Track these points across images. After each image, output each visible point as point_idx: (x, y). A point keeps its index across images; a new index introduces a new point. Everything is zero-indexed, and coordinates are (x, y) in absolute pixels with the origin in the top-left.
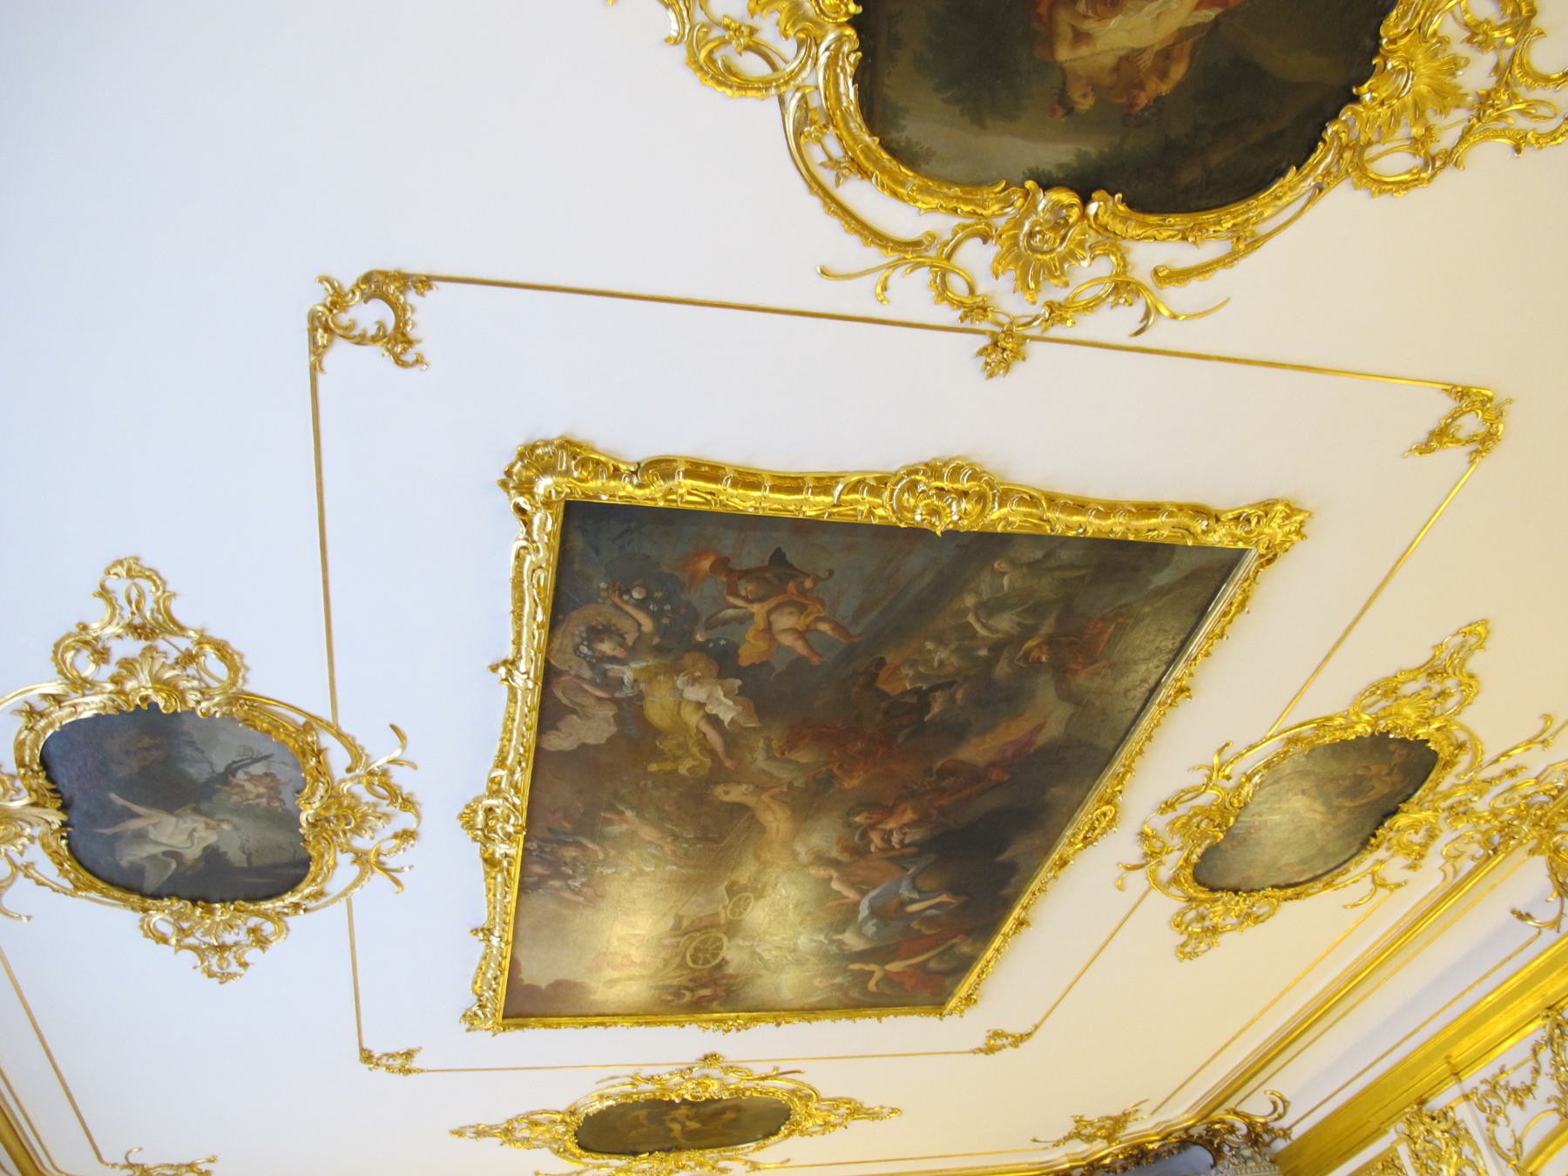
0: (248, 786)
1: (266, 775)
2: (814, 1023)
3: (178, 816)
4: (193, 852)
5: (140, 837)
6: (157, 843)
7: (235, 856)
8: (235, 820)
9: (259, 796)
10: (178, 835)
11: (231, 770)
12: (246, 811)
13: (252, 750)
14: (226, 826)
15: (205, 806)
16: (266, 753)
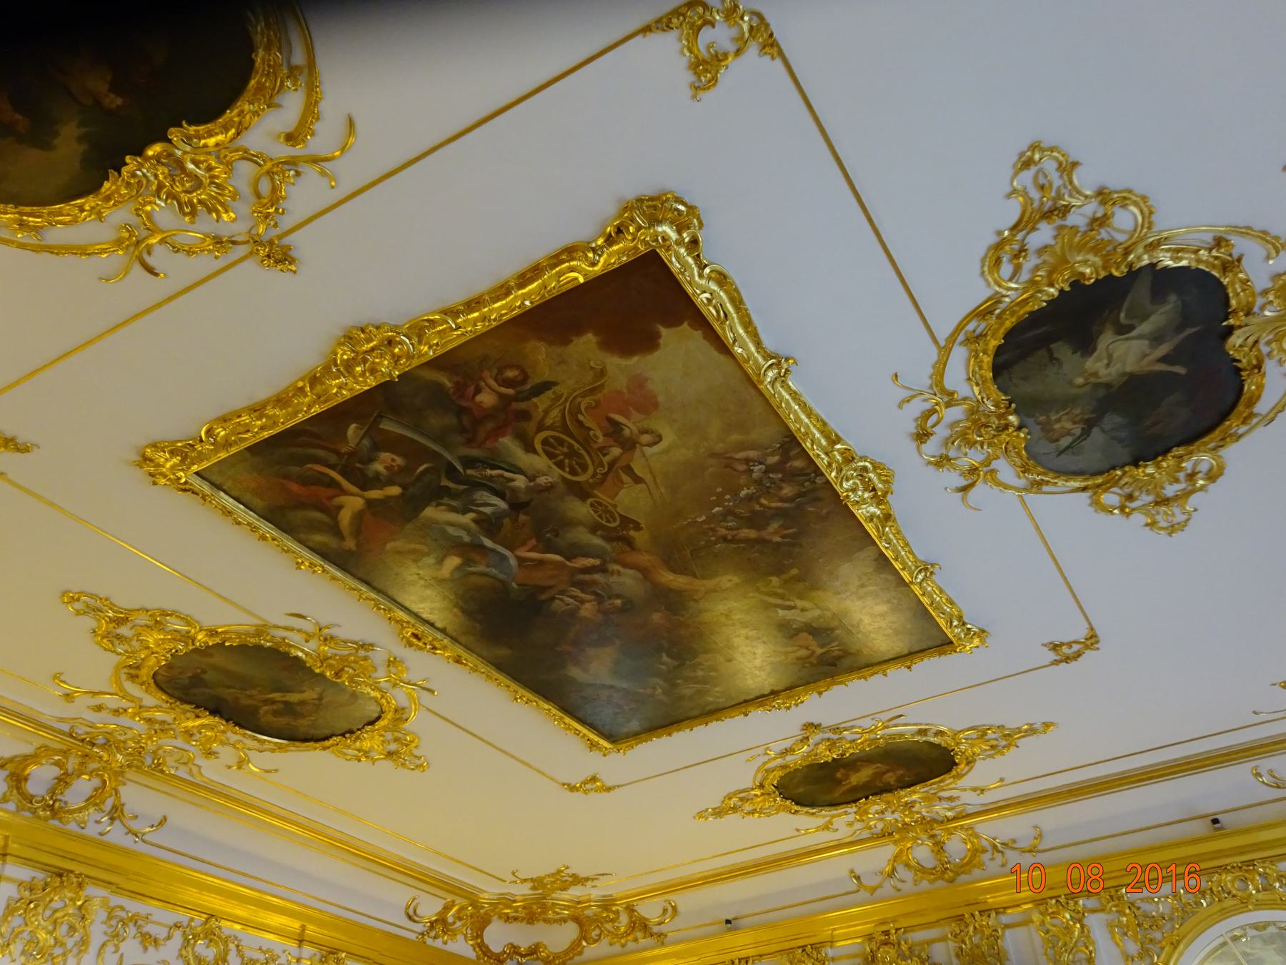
0: (1069, 425)
1: (1057, 440)
2: (675, 735)
3: (1124, 374)
4: (1107, 340)
5: (1156, 339)
6: (1139, 337)
7: (1063, 350)
8: (1073, 391)
9: (1059, 420)
10: (1123, 354)
11: (1086, 433)
12: (1066, 402)
13: (1073, 453)
14: (1080, 381)
15: (1101, 393)
16: (1063, 456)
